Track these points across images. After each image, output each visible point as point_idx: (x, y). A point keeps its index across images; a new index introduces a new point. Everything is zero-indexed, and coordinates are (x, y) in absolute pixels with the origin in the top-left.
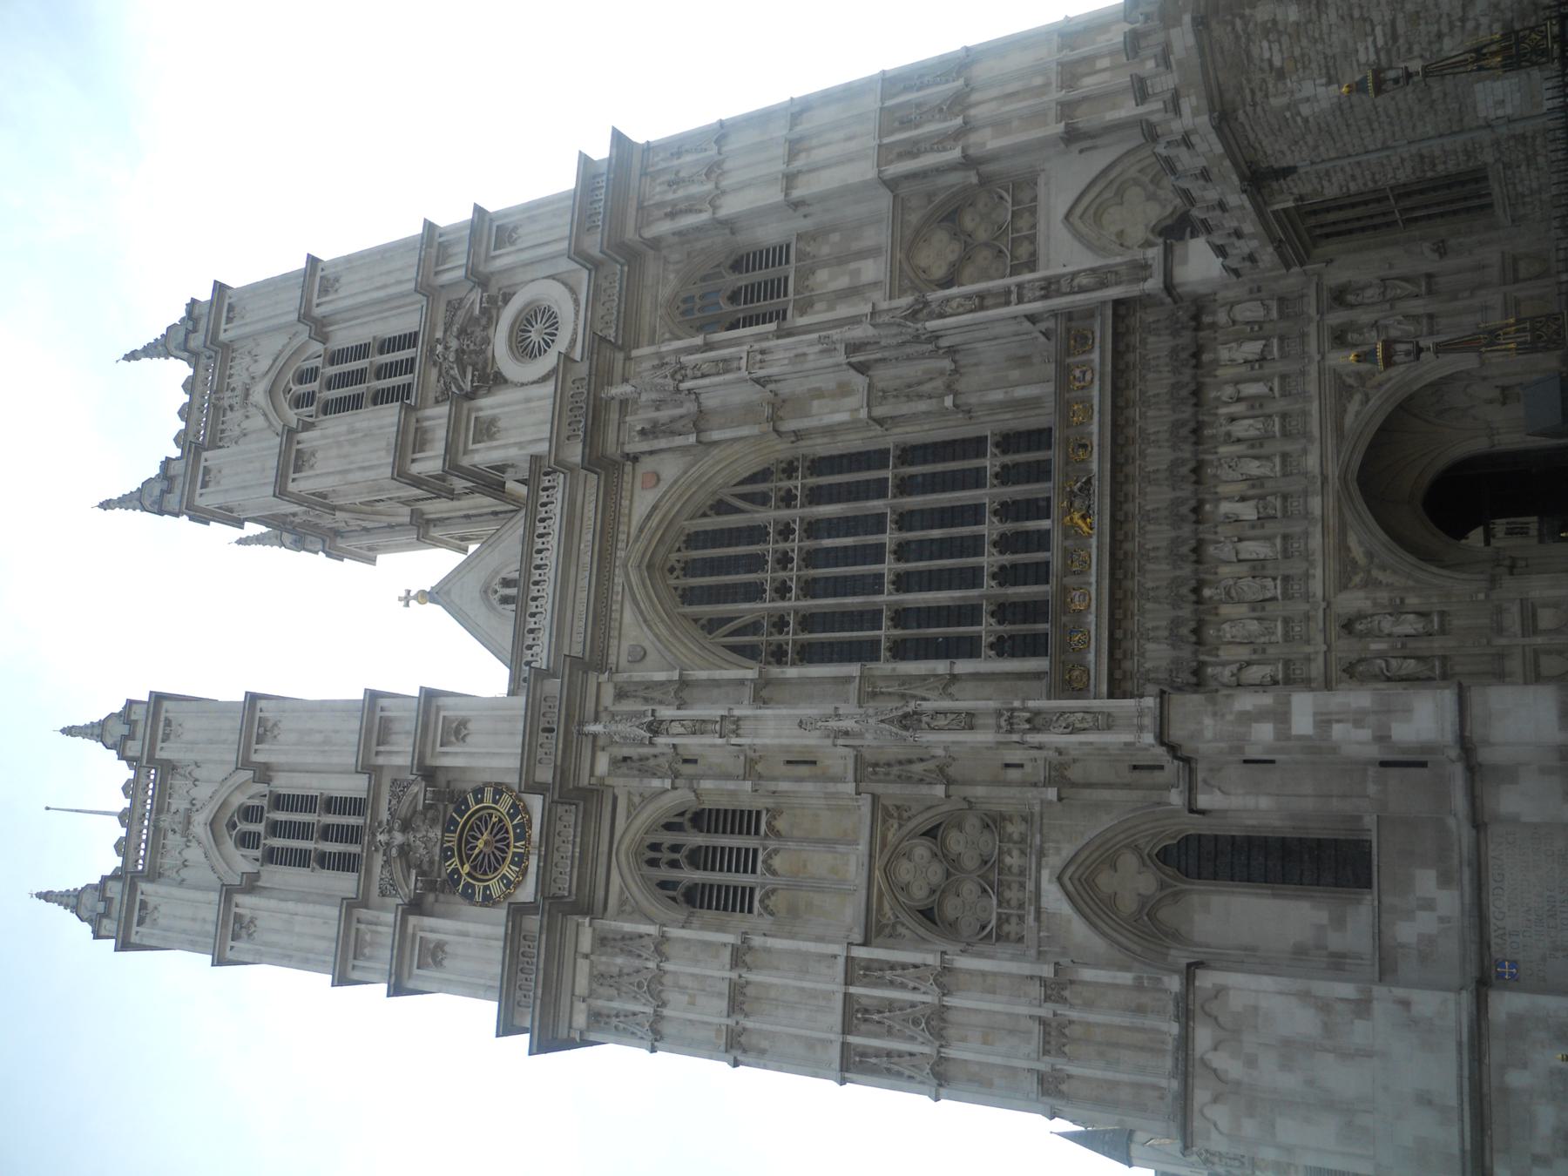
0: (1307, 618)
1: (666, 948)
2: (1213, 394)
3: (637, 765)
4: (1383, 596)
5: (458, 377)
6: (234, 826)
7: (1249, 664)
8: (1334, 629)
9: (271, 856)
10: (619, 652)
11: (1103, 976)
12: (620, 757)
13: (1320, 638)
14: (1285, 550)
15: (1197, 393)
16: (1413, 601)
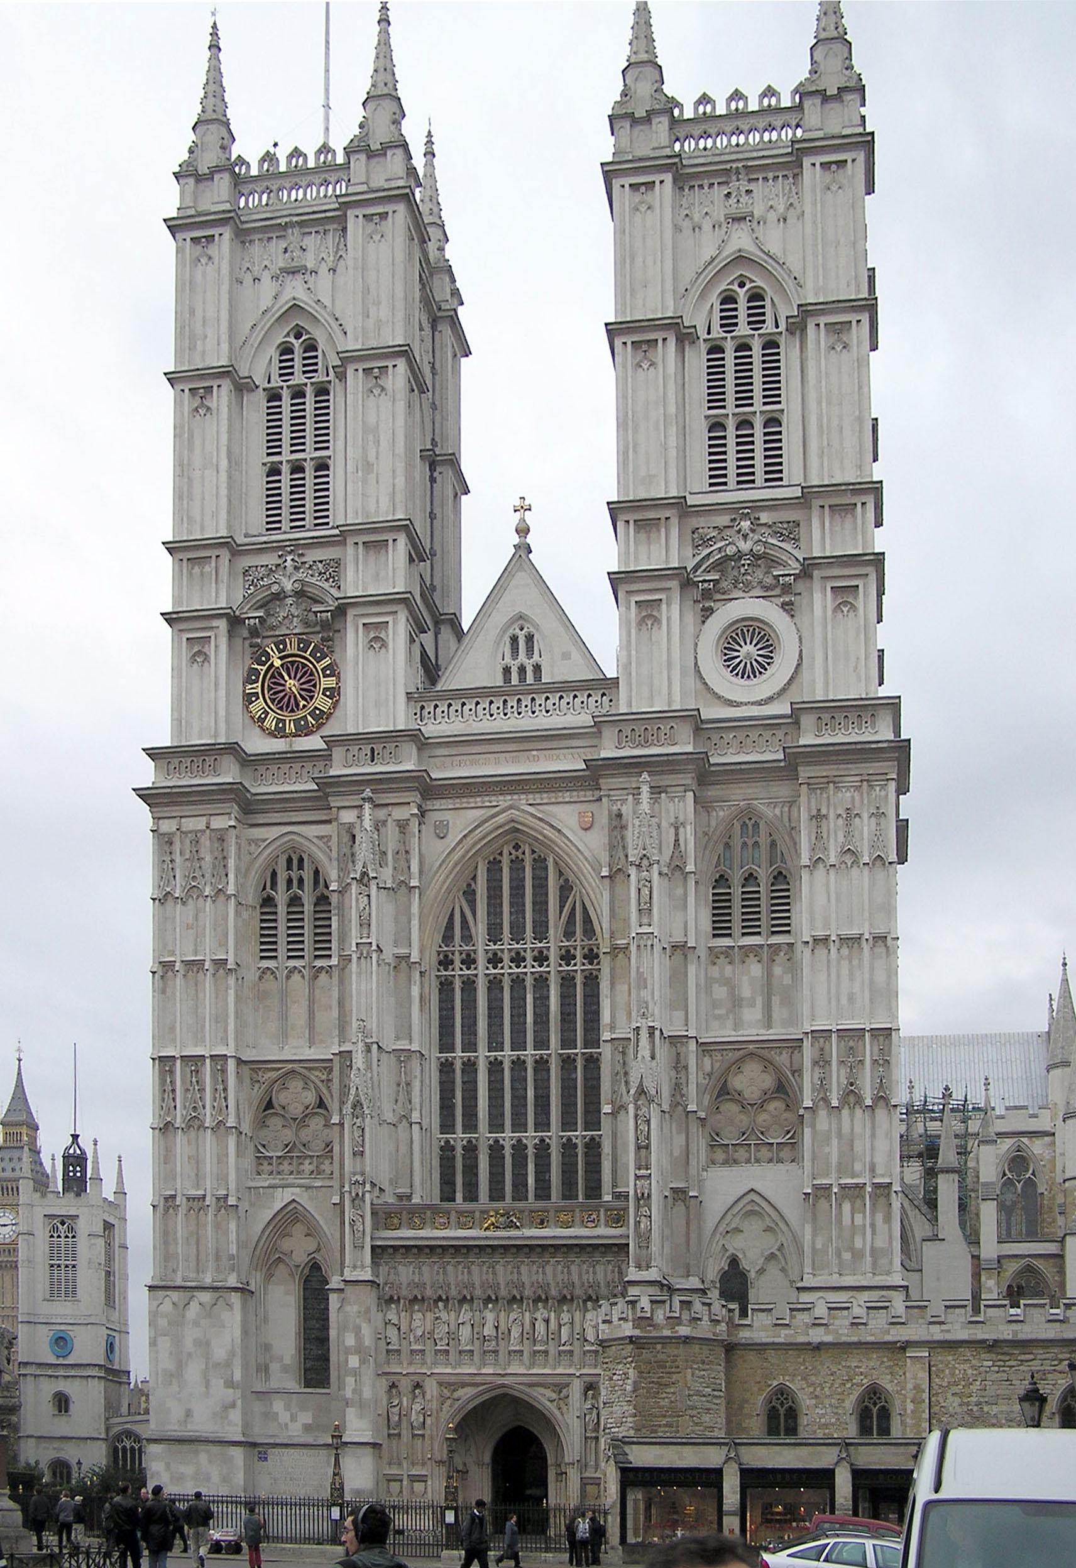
0: (424, 1363)
1: (222, 898)
2: (565, 1308)
3: (349, 853)
4: (435, 1405)
5: (711, 561)
6: (298, 337)
7: (399, 1329)
8: (416, 1378)
9: (274, 396)
10: (442, 811)
11: (233, 1236)
12: (356, 832)
13: (411, 1370)
14: (465, 1351)
15: (563, 1300)
16: (429, 1421)
